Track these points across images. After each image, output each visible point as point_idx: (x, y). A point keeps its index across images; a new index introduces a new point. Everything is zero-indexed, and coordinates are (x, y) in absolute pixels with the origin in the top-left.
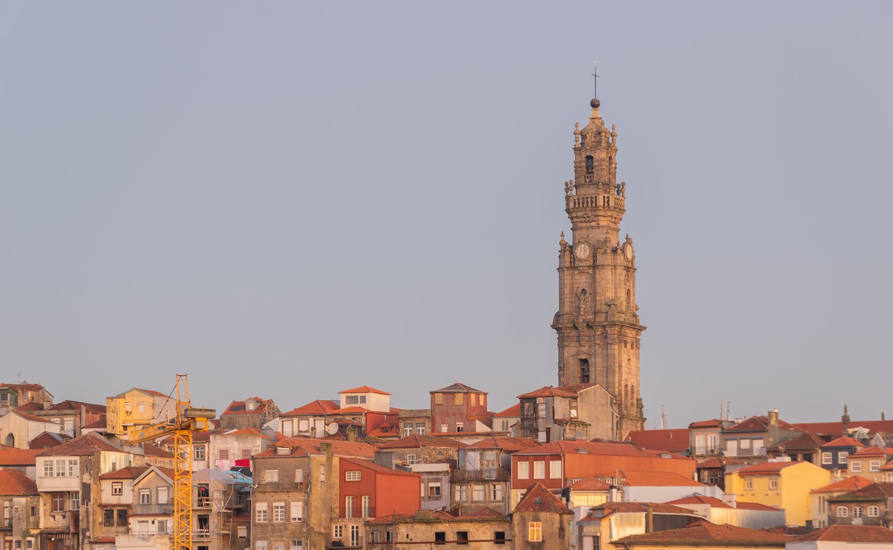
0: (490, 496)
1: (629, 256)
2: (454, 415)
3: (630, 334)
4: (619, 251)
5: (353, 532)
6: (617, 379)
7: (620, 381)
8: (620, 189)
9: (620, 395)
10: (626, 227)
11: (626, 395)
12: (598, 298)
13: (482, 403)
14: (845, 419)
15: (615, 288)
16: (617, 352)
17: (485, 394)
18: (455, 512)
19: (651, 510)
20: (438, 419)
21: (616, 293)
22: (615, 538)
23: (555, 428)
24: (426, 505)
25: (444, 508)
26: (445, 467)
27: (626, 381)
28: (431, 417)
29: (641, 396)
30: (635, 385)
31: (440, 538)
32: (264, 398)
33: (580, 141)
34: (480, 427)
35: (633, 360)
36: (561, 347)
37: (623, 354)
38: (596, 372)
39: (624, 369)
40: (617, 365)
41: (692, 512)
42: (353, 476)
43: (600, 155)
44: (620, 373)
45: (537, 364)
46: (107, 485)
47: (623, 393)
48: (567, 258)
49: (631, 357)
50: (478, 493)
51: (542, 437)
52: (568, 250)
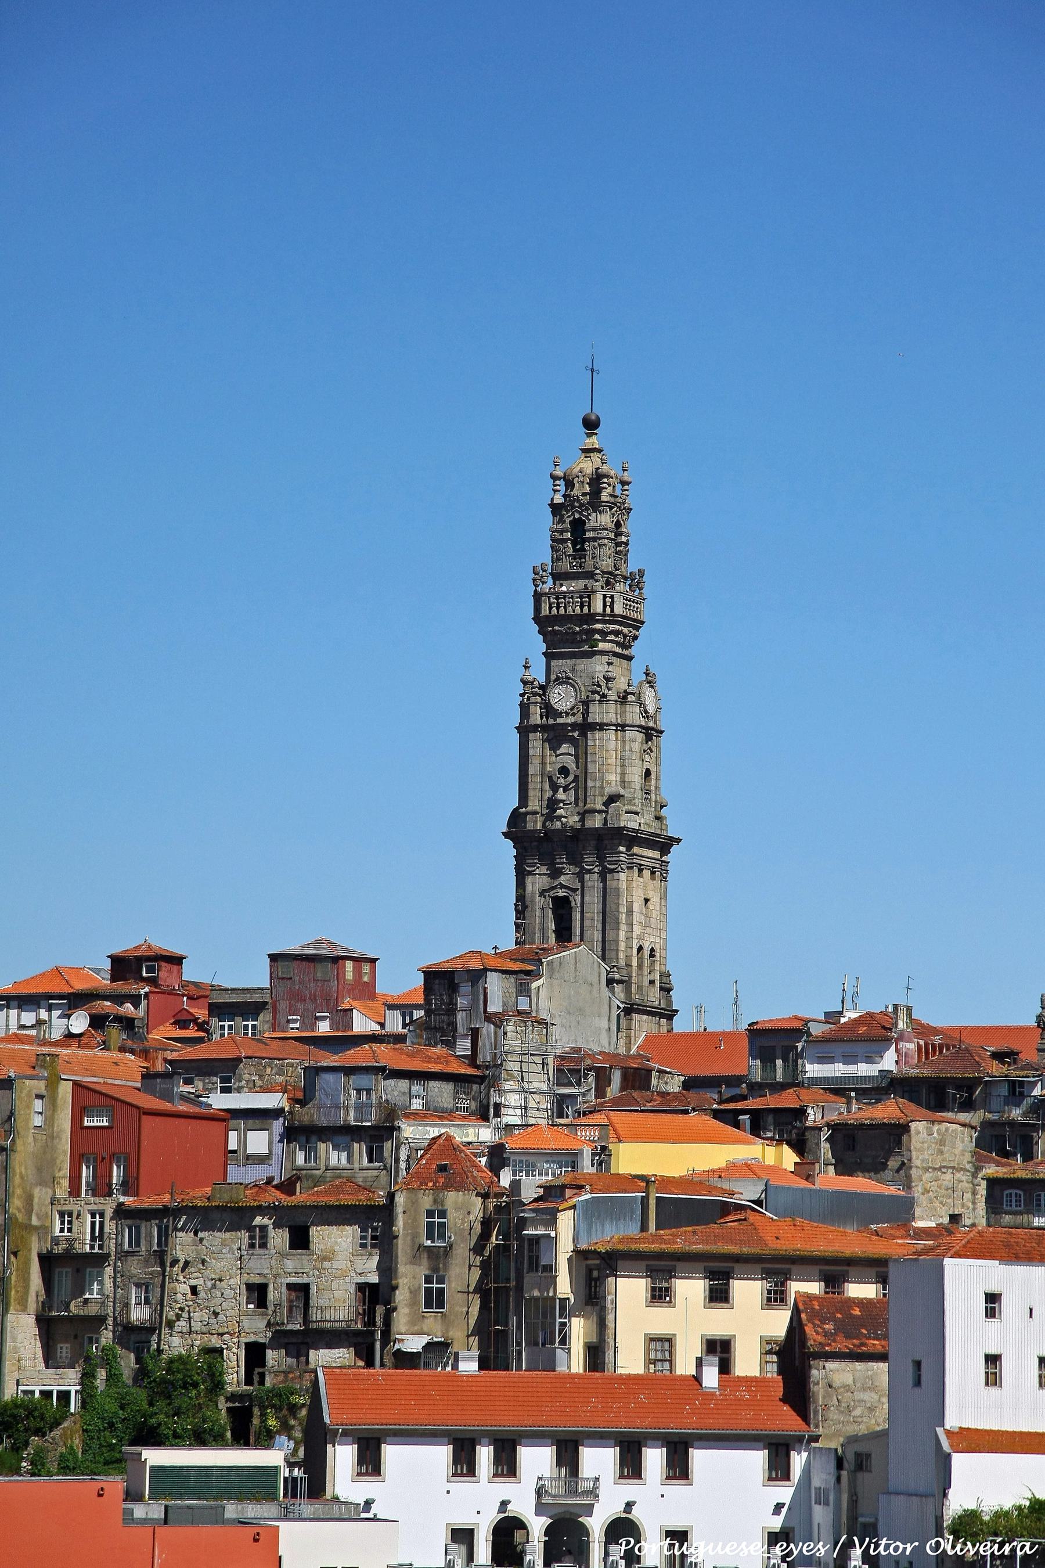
0: (361, 1156)
1: (651, 709)
2: (313, 998)
4: (630, 698)
5: (93, 1224)
6: (622, 935)
7: (629, 939)
8: (636, 581)
9: (629, 965)
11: (640, 966)
12: (590, 784)
13: (366, 979)
15: (623, 766)
16: (623, 885)
17: (373, 961)
19: (652, 1189)
20: (283, 1005)
21: (623, 774)
22: (583, 1246)
23: (488, 1030)
24: (236, 1174)
25: (270, 1180)
27: (640, 938)
29: (669, 968)
30: (657, 947)
33: (563, 492)
35: (655, 899)
36: (521, 875)
37: (634, 887)
39: (637, 917)
40: (623, 909)
41: (732, 1194)
44: (630, 925)
45: (474, 907)
47: (634, 963)
48: (536, 712)
49: (650, 894)
51: (463, 1047)
52: (535, 694)
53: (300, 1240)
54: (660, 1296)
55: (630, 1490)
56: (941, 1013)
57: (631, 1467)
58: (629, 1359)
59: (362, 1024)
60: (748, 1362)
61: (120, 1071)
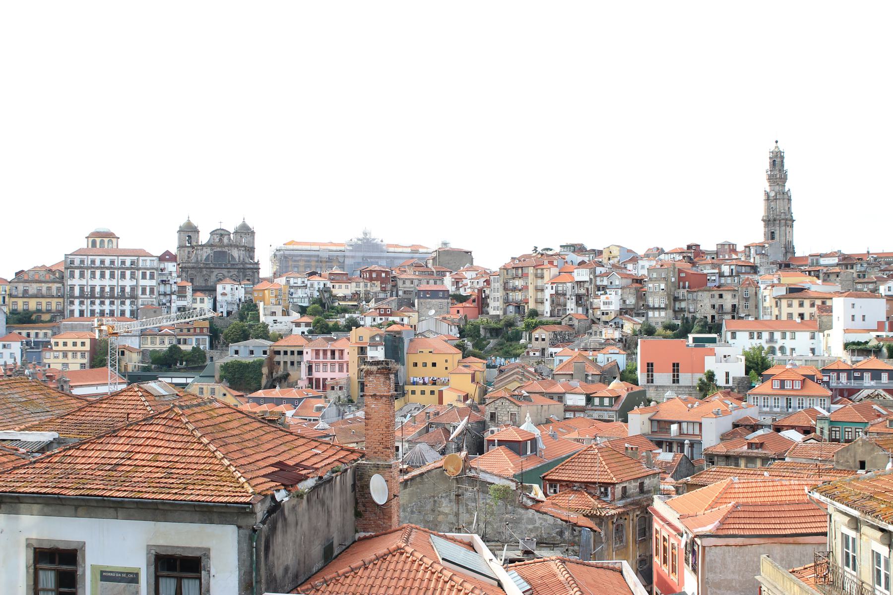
3: (789, 222)
10: (788, 185)
14: (868, 252)
18: (719, 287)
26: (716, 271)
28: (717, 253)
31: (713, 296)
32: (660, 247)
34: (734, 256)
38: (777, 236)
42: (683, 275)
43: (778, 160)
46: (598, 279)
50: (729, 280)
51: (752, 260)
52: (767, 194)
53: (721, 296)
54: (790, 306)
55: (784, 341)
56: (847, 251)
57: (784, 337)
58: (784, 317)
59: (734, 256)
60: (807, 317)
61: (687, 266)
